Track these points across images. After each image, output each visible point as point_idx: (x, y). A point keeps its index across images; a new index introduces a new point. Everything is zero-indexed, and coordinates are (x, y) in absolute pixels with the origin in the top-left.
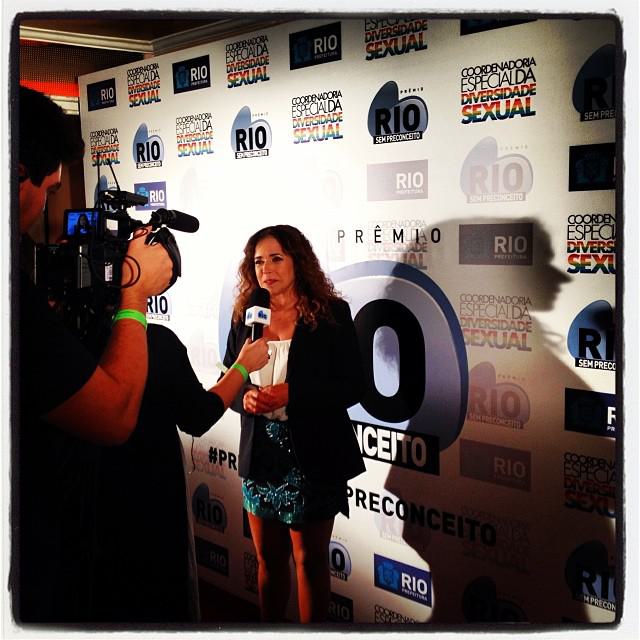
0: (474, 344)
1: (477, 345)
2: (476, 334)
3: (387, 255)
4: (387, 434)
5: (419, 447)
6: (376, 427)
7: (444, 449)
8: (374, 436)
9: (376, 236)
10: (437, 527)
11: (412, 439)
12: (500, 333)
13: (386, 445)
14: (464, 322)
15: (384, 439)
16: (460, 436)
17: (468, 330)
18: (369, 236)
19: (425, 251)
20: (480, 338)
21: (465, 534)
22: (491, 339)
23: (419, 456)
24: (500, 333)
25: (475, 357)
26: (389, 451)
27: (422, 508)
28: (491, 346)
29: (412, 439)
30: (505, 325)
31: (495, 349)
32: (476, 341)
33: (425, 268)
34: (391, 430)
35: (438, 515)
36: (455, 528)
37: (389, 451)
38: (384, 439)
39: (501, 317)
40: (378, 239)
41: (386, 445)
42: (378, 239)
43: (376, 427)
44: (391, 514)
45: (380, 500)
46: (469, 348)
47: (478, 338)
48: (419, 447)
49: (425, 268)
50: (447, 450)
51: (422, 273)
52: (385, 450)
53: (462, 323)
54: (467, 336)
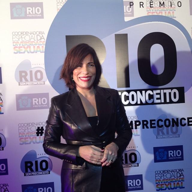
3: (157, 13)
4: (158, 91)
5: (175, 93)
6: (152, 90)
8: (151, 93)
9: (150, 5)
10: (185, 125)
11: (171, 90)
13: (158, 96)
15: (157, 94)
19: (174, 10)
23: (175, 97)
26: (160, 98)
29: (171, 90)
33: (175, 17)
34: (160, 89)
37: (160, 98)
38: (157, 94)
41: (158, 96)
44: (162, 126)
45: (156, 122)
48: (175, 93)
49: (175, 17)
50: (187, 92)
52: (157, 99)
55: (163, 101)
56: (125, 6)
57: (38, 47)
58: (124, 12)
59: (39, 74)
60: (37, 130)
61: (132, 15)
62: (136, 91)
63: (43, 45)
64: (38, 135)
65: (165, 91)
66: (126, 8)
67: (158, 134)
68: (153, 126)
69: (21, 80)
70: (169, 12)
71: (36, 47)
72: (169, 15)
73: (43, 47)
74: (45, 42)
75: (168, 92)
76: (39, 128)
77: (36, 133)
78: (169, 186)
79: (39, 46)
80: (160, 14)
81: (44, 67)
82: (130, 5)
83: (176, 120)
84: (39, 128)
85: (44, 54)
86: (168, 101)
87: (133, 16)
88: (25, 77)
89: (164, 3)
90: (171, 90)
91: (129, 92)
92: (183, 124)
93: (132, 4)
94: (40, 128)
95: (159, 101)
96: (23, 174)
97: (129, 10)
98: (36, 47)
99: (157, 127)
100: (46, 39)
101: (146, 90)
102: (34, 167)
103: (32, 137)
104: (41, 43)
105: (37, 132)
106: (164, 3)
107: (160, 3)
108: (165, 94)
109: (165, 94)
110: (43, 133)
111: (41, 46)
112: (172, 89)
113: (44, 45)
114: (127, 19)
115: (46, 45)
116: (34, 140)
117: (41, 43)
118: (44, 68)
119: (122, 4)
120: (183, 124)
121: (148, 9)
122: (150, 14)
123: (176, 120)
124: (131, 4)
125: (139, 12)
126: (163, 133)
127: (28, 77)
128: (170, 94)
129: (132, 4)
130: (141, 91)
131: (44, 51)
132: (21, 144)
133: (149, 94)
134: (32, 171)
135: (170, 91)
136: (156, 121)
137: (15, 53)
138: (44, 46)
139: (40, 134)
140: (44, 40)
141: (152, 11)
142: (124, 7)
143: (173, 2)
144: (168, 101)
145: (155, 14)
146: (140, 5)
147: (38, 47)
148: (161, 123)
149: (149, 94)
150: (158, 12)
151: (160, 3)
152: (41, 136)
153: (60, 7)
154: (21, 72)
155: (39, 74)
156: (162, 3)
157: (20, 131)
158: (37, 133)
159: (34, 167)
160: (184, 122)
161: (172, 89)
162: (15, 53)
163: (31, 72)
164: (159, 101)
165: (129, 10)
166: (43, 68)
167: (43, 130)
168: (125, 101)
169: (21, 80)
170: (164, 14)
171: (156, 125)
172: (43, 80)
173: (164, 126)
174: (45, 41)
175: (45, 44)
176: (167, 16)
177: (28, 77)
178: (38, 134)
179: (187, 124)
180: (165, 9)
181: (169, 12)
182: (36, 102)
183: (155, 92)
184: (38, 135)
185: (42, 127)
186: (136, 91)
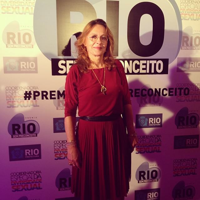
1: (186, 20)
2: (186, 16)
4: (145, 62)
5: (160, 65)
6: (139, 60)
7: (170, 63)
8: (138, 63)
11: (157, 62)
12: (195, 14)
13: (144, 67)
15: (143, 64)
16: (178, 57)
17: (183, 14)
20: (188, 17)
21: (177, 94)
22: (192, 17)
23: (159, 68)
24: (195, 14)
26: (145, 69)
27: (160, 89)
28: (192, 20)
29: (157, 62)
30: (197, 12)
31: (193, 21)
32: (186, 18)
34: (147, 60)
37: (145, 69)
38: (143, 64)
39: (196, 9)
41: (144, 67)
43: (139, 60)
44: (145, 95)
46: (183, 21)
47: (187, 17)
48: (160, 65)
52: (143, 69)
53: (181, 11)
54: (183, 17)
55: (148, 72)
57: (27, 8)
59: (27, 37)
60: (25, 94)
63: (32, 7)
64: (26, 99)
65: (151, 62)
69: (9, 42)
71: (25, 8)
73: (32, 8)
74: (35, 4)
75: (153, 62)
76: (26, 92)
77: (23, 97)
79: (28, 8)
81: (32, 29)
83: (158, 90)
84: (26, 92)
85: (33, 16)
86: (153, 71)
88: (13, 39)
92: (165, 94)
95: (144, 71)
96: (11, 136)
98: (25, 8)
99: (140, 96)
101: (133, 60)
102: (21, 130)
103: (19, 101)
104: (30, 4)
105: (25, 96)
108: (151, 65)
109: (151, 65)
110: (31, 97)
111: (30, 8)
112: (157, 60)
113: (33, 6)
115: (35, 6)
117: (30, 4)
118: (33, 31)
123: (158, 90)
127: (16, 40)
128: (155, 64)
130: (128, 60)
131: (33, 12)
132: (8, 107)
133: (136, 64)
134: (19, 133)
135: (155, 62)
137: (2, 13)
138: (34, 8)
139: (27, 98)
144: (153, 71)
147: (27, 8)
149: (136, 64)
152: (29, 100)
154: (9, 34)
155: (27, 37)
157: (7, 94)
158: (24, 97)
159: (21, 130)
161: (157, 60)
162: (2, 13)
163: (19, 34)
164: (144, 71)
166: (31, 31)
167: (31, 94)
169: (9, 42)
171: (140, 94)
172: (31, 44)
173: (147, 95)
174: (35, 2)
175: (34, 5)
177: (16, 40)
182: (24, 66)
183: (142, 62)
184: (26, 99)
185: (30, 92)
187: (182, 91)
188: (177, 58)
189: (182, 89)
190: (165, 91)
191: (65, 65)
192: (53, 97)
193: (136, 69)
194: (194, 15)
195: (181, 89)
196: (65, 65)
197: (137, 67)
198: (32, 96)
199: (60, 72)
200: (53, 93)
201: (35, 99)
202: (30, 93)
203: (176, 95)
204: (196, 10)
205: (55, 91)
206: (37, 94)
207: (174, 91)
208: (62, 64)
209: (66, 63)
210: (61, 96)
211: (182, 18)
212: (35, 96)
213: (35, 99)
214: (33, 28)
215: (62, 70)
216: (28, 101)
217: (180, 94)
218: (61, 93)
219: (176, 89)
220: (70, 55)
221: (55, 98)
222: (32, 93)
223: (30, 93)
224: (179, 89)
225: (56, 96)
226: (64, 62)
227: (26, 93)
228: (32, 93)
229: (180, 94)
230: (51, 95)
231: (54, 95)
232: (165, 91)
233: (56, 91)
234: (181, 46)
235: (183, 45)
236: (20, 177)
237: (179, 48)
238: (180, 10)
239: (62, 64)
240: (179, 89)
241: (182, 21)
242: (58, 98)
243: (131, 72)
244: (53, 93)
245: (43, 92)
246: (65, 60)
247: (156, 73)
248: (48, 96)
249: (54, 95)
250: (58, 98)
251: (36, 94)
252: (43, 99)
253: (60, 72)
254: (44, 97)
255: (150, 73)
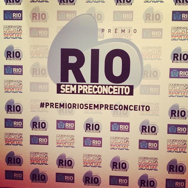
0: (145, 59)
4: (117, 87)
5: (127, 89)
6: (113, 86)
7: (137, 87)
8: (112, 88)
10: (132, 110)
13: (116, 90)
14: (143, 54)
15: (116, 88)
18: (113, 31)
19: (131, 35)
21: (140, 109)
23: (127, 91)
25: (145, 63)
26: (117, 92)
27: (127, 106)
33: (131, 40)
34: (118, 86)
35: (132, 106)
36: (138, 109)
37: (117, 92)
38: (116, 88)
40: (116, 32)
41: (116, 90)
42: (116, 32)
43: (113, 86)
44: (117, 109)
45: (113, 106)
48: (127, 89)
49: (131, 40)
51: (130, 41)
52: (116, 92)
54: (143, 57)
55: (119, 93)
56: (99, 32)
58: (98, 35)
61: (103, 38)
62: (102, 85)
64: (41, 107)
65: (121, 87)
66: (100, 33)
67: (114, 114)
68: (111, 108)
70: (127, 37)
72: (127, 38)
75: (122, 87)
78: (119, 147)
80: (121, 38)
82: (102, 31)
84: (42, 103)
85: (47, 59)
86: (122, 93)
87: (104, 38)
89: (124, 30)
90: (125, 87)
91: (98, 85)
92: (131, 109)
93: (103, 30)
94: (43, 103)
95: (116, 93)
97: (101, 34)
99: (114, 109)
100: (49, 50)
101: (109, 86)
106: (124, 30)
107: (122, 30)
108: (121, 89)
109: (121, 89)
110: (44, 106)
111: (46, 54)
112: (125, 86)
114: (99, 40)
116: (39, 110)
118: (47, 67)
119: (96, 29)
120: (131, 109)
121: (114, 34)
122: (115, 37)
124: (103, 30)
125: (107, 36)
126: (117, 114)
128: (124, 89)
129: (103, 30)
130: (105, 86)
131: (48, 57)
135: (124, 87)
136: (114, 105)
138: (48, 54)
140: (48, 51)
141: (116, 35)
142: (98, 32)
143: (131, 30)
144: (122, 93)
145: (118, 37)
146: (109, 31)
148: (116, 107)
150: (120, 36)
151: (122, 30)
153: (59, 31)
156: (123, 30)
160: (131, 108)
161: (125, 86)
164: (116, 93)
165: (101, 34)
168: (95, 91)
170: (124, 38)
171: (113, 108)
173: (118, 109)
176: (126, 39)
178: (41, 106)
179: (133, 110)
180: (125, 34)
181: (127, 37)
183: (115, 87)
184: (41, 107)
185: (44, 103)
186: (102, 85)
187: (145, 108)
188: (139, 85)
189: (144, 106)
190: (131, 107)
191: (65, 87)
192: (57, 107)
193: (111, 91)
194: (152, 56)
195: (143, 106)
196: (65, 87)
197: (111, 90)
198: (45, 105)
199: (62, 91)
200: (57, 104)
201: (46, 107)
202: (44, 104)
203: (139, 110)
204: (154, 53)
205: (58, 103)
206: (47, 104)
207: (138, 107)
208: (63, 87)
209: (65, 86)
210: (62, 107)
211: (143, 58)
212: (46, 106)
213: (46, 107)
214: (47, 66)
215: (63, 90)
216: (42, 109)
217: (143, 110)
218: (62, 104)
219: (139, 106)
220: (68, 81)
221: (58, 108)
222: (45, 104)
223: (44, 104)
224: (141, 106)
225: (59, 106)
226: (64, 86)
227: (41, 104)
228: (45, 104)
229: (143, 110)
230: (56, 105)
231: (58, 106)
232: (131, 107)
233: (59, 104)
234: (143, 77)
235: (144, 76)
236: (35, 155)
237: (141, 78)
238: (141, 53)
239: (63, 87)
240: (141, 106)
241: (143, 60)
242: (60, 108)
243: (107, 93)
244: (57, 104)
245: (51, 103)
246: (65, 84)
247: (124, 94)
248: (54, 106)
249: (58, 106)
250: (60, 108)
251: (47, 104)
252: (51, 107)
253: (62, 91)
254: (52, 106)
255: (120, 94)
